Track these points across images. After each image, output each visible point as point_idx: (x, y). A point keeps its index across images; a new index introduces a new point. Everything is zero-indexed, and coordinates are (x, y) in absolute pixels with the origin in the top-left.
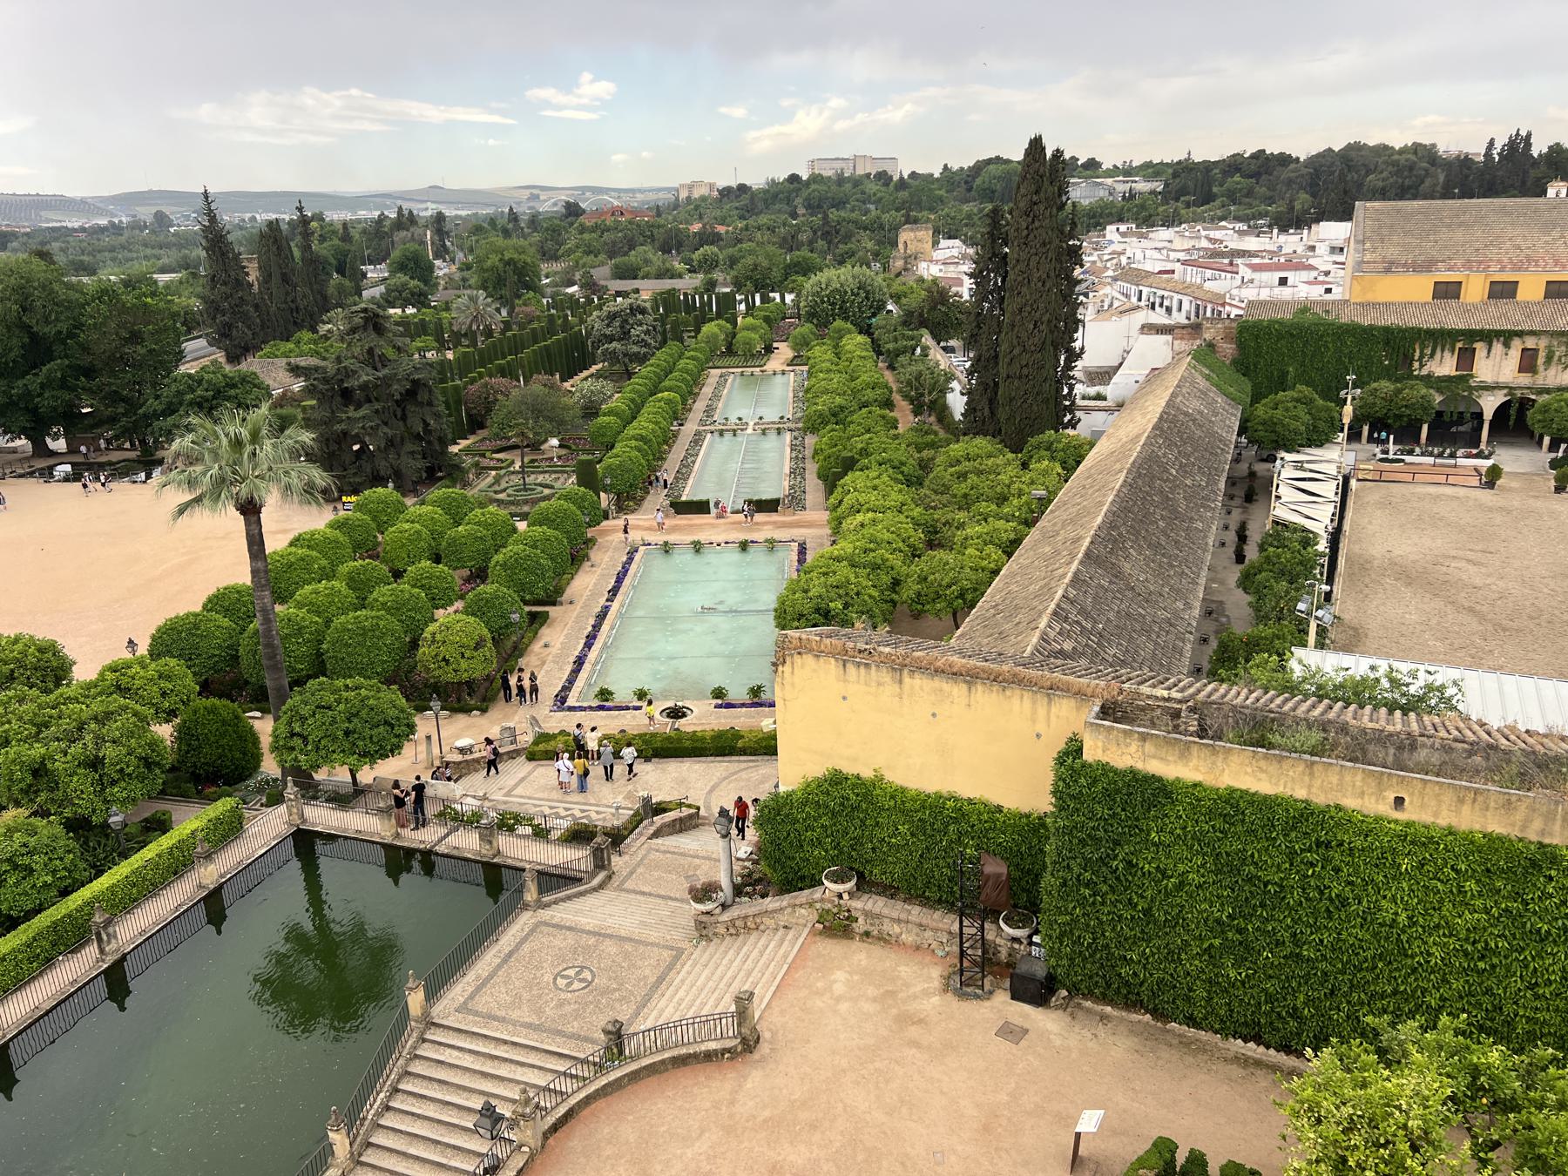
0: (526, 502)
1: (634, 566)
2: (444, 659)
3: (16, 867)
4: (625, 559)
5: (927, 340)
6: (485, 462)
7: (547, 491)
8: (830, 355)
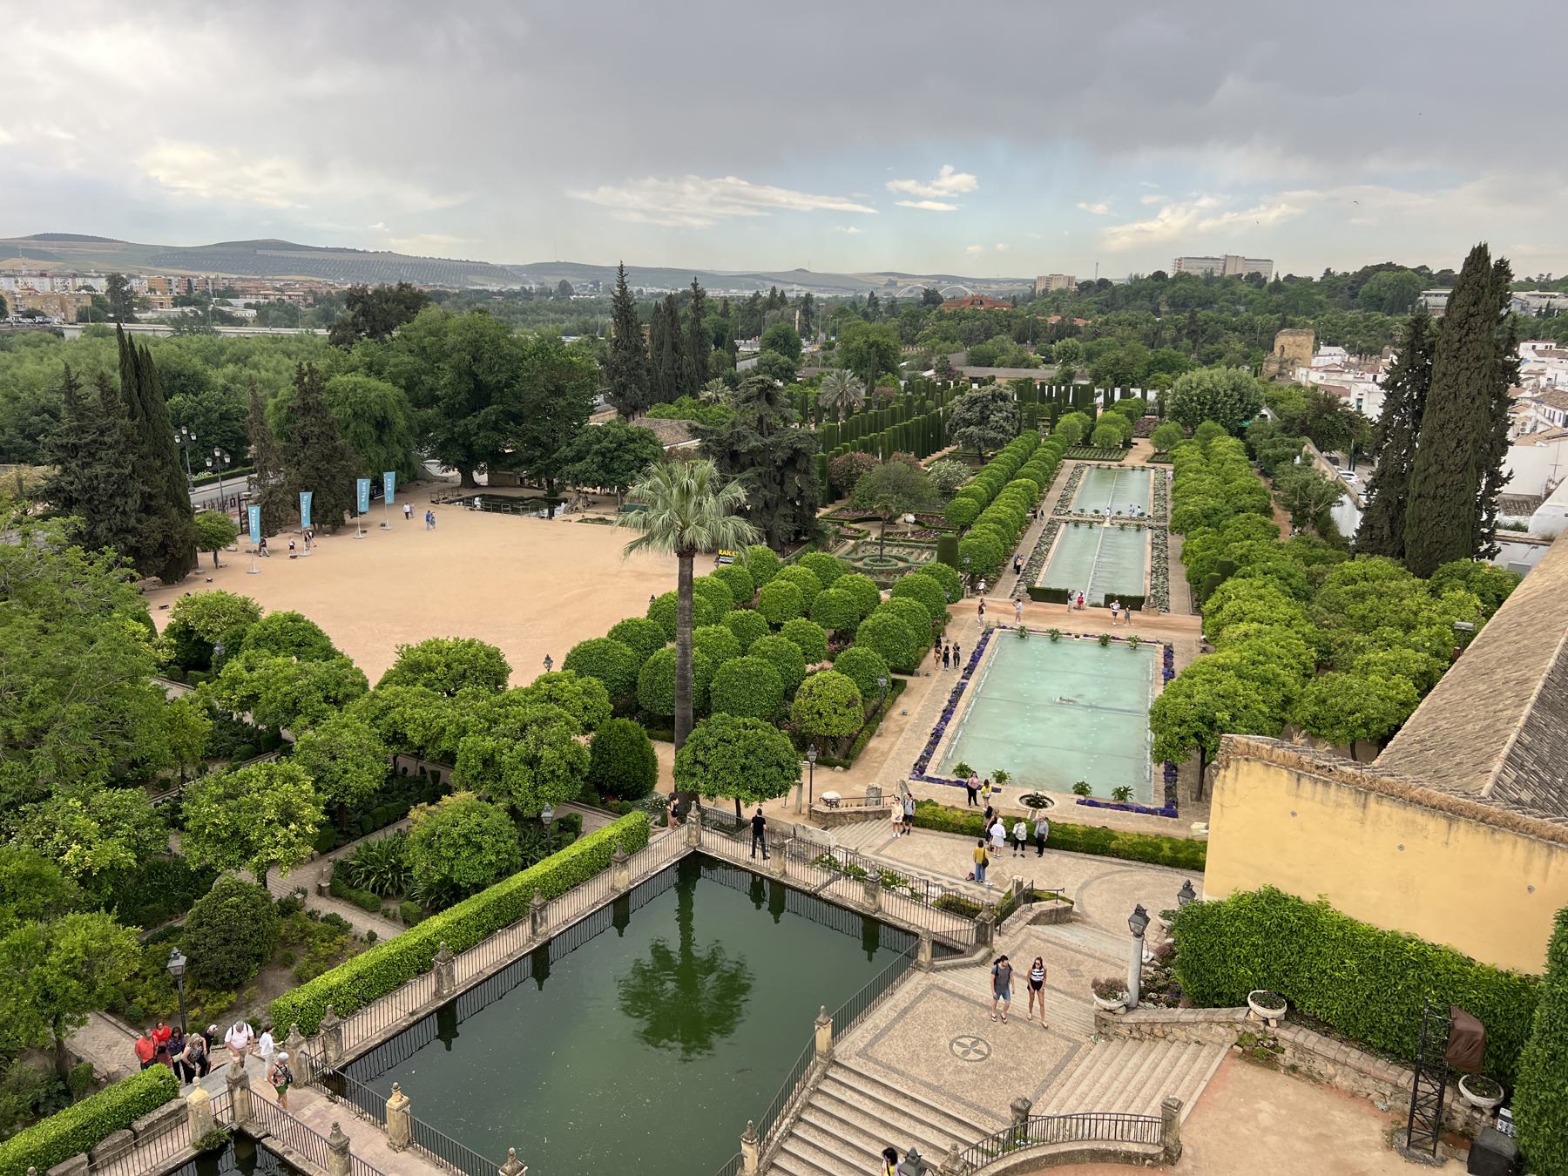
0: (882, 572)
1: (988, 649)
3: (469, 842)
4: (980, 638)
5: (1310, 448)
6: (844, 531)
7: (901, 565)
8: (1198, 455)
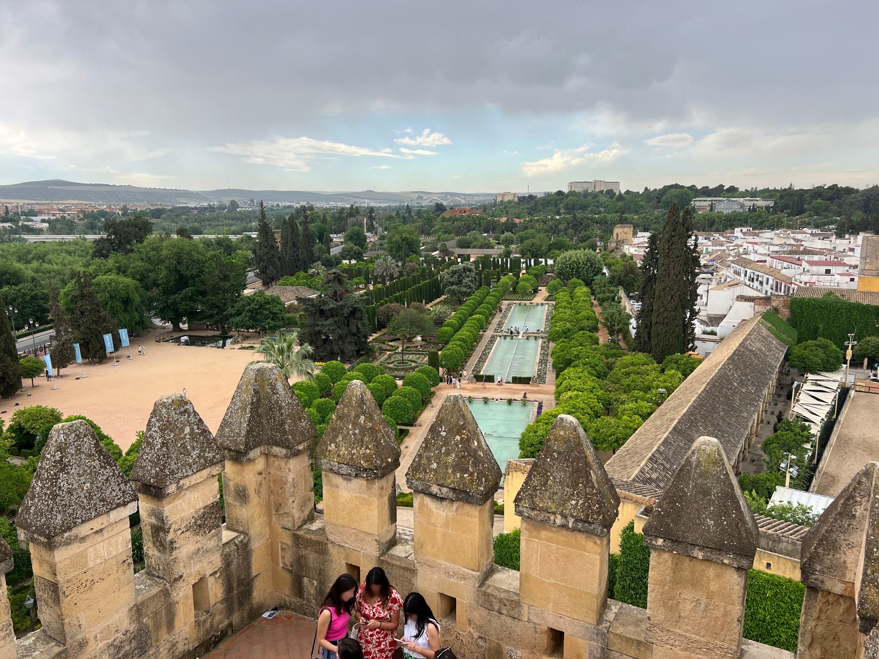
0: (403, 369)
5: (622, 293)
6: (384, 347)
7: (413, 364)
8: (567, 298)
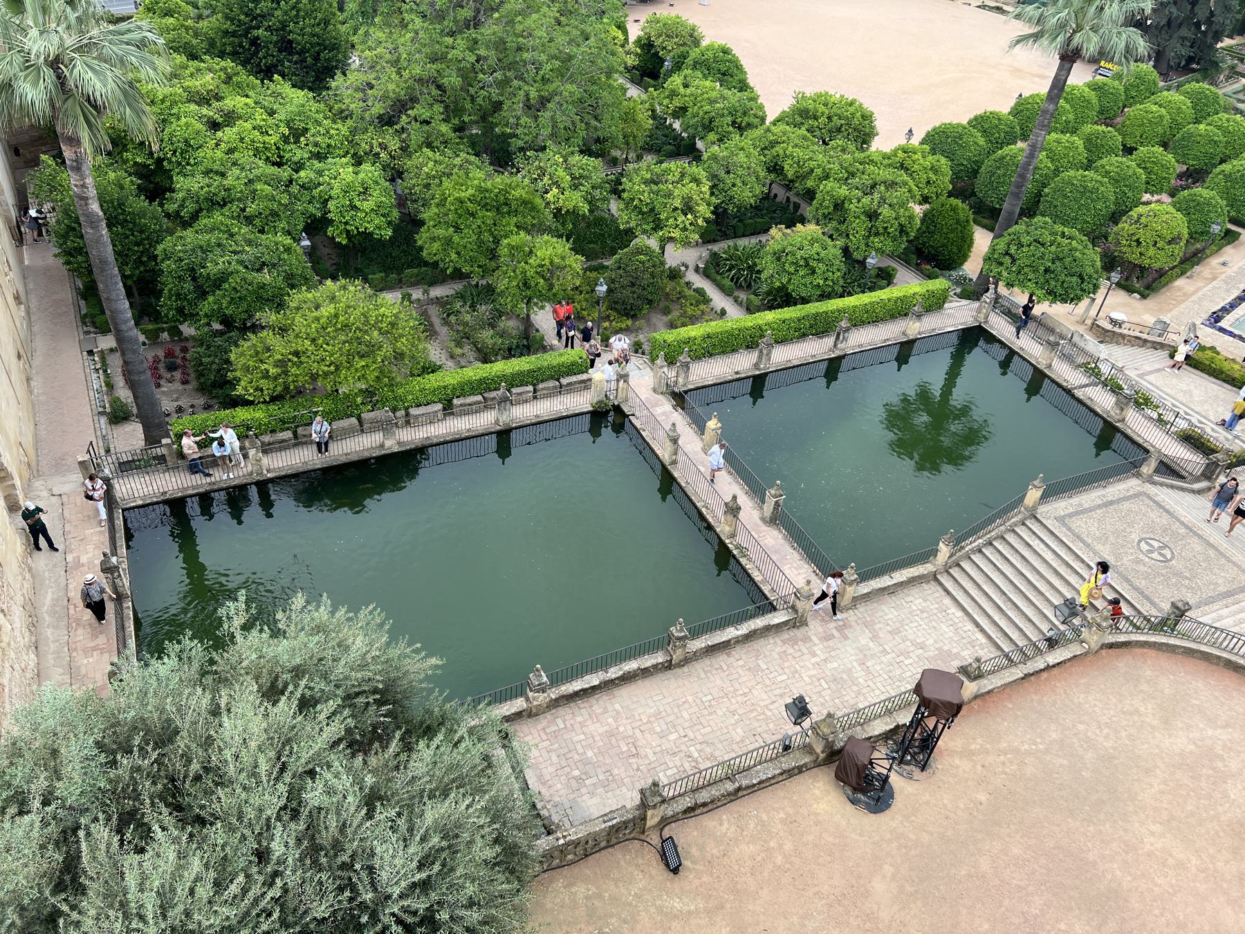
2: (1137, 241)
3: (807, 265)
